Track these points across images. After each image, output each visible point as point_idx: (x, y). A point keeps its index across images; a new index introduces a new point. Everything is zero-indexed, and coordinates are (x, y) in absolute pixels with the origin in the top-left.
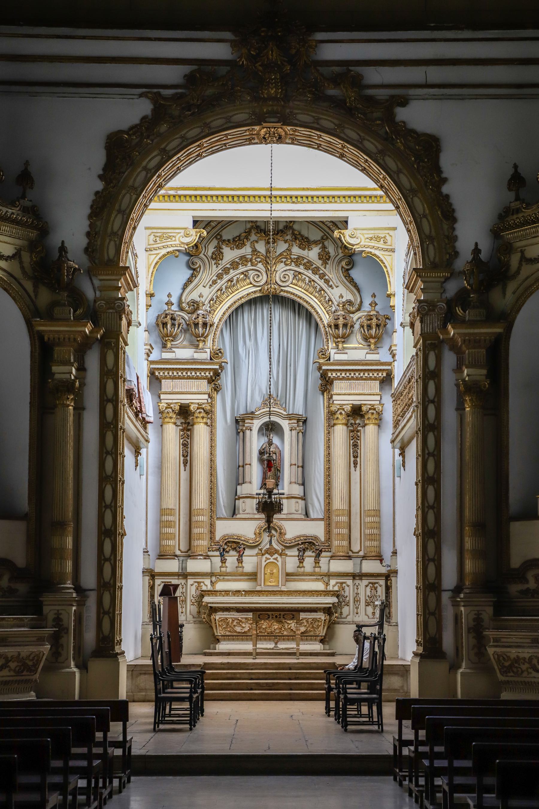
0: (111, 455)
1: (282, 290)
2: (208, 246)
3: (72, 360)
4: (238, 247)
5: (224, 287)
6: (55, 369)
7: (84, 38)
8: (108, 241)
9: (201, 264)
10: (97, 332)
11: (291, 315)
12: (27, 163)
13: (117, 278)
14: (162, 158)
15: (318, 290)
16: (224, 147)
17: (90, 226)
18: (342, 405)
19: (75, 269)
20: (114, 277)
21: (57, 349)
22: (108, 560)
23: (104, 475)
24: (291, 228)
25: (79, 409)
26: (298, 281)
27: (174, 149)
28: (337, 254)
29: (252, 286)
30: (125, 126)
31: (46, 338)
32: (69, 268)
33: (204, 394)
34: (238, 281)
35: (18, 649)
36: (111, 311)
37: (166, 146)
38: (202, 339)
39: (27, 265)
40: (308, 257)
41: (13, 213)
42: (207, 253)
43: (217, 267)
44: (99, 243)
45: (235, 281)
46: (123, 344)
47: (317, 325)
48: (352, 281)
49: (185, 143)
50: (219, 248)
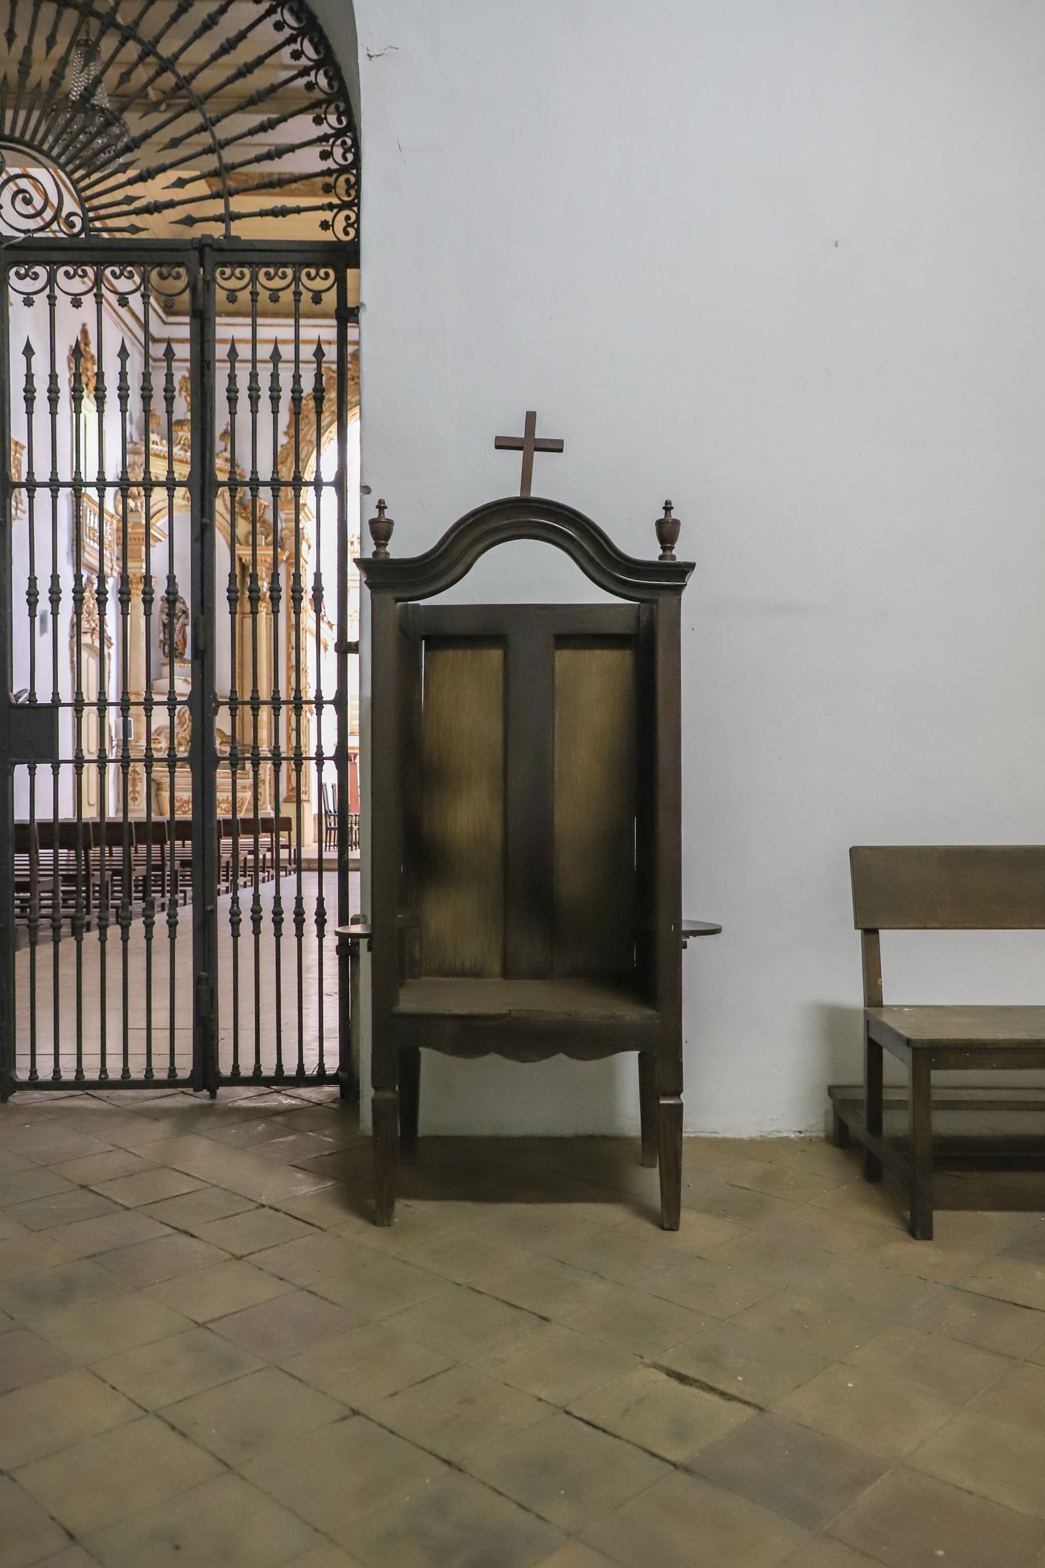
3: (264, 576)
7: (271, 325)
14: (332, 419)
19: (265, 506)
23: (290, 665)
31: (244, 561)
32: (261, 505)
46: (304, 563)
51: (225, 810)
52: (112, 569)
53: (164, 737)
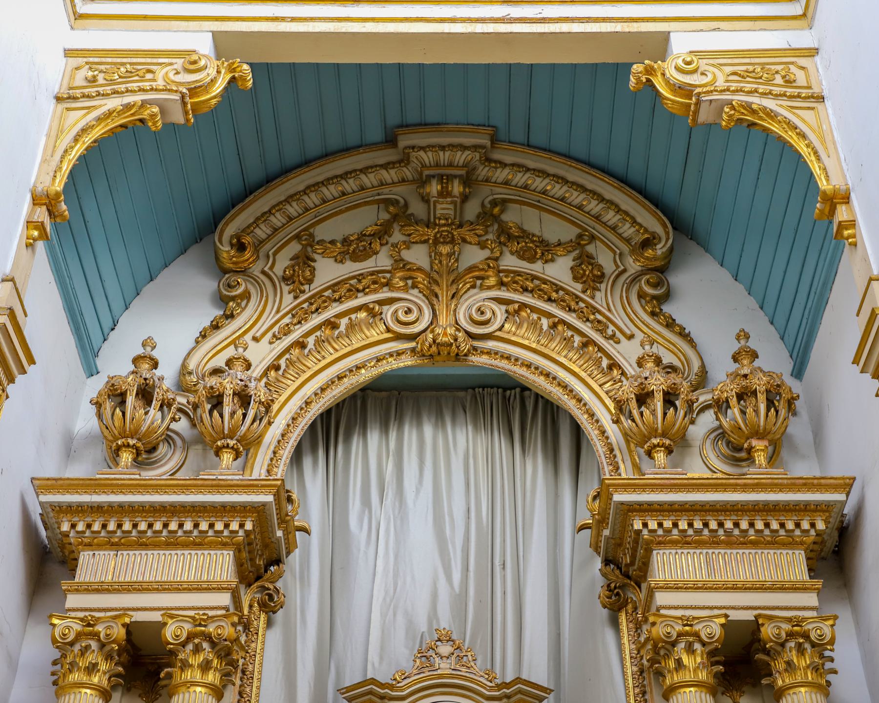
1: (475, 349)
2: (275, 254)
4: (356, 257)
5: (311, 340)
9: (250, 287)
11: (500, 443)
15: (576, 345)
18: (687, 622)
24: (496, 218)
26: (519, 326)
28: (622, 268)
29: (389, 335)
33: (220, 589)
34: (351, 326)
38: (232, 443)
40: (543, 274)
42: (271, 268)
43: (296, 298)
45: (342, 328)
47: (577, 431)
48: (670, 324)
50: (304, 260)
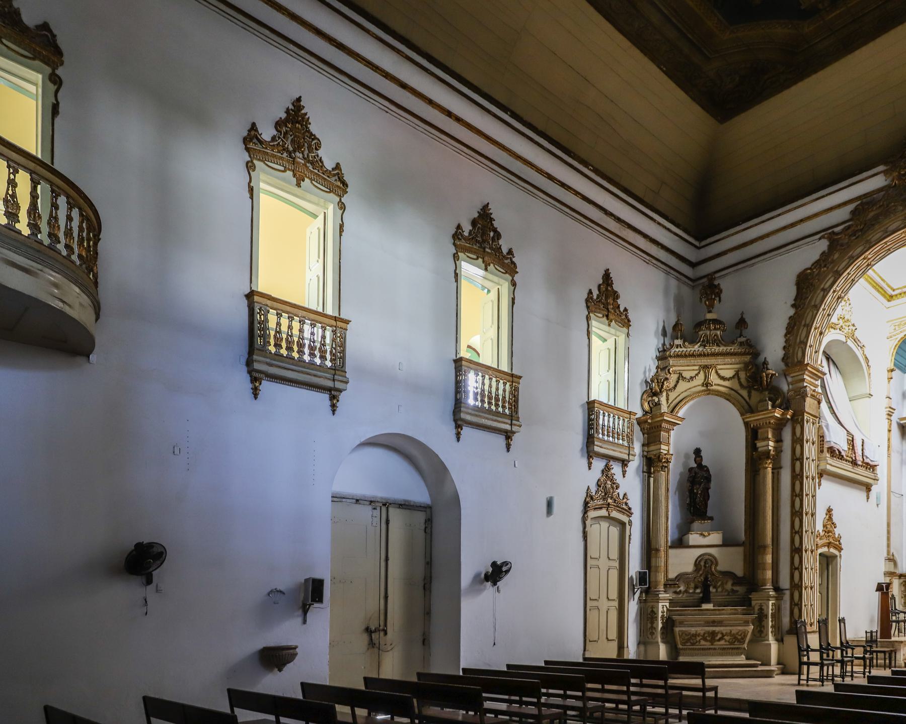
0: (799, 496)
6: (759, 444)
8: (797, 348)
10: (787, 414)
12: (742, 314)
13: (803, 372)
16: (889, 252)
17: (786, 342)
19: (772, 375)
20: (800, 373)
21: (760, 431)
22: (797, 569)
23: (794, 511)
25: (777, 469)
27: (843, 268)
30: (809, 265)
35: (729, 628)
36: (798, 397)
37: (838, 268)
39: (743, 380)
41: (731, 349)
44: (791, 351)
49: (852, 261)
51: (729, 642)
52: (629, 455)
53: (683, 582)
